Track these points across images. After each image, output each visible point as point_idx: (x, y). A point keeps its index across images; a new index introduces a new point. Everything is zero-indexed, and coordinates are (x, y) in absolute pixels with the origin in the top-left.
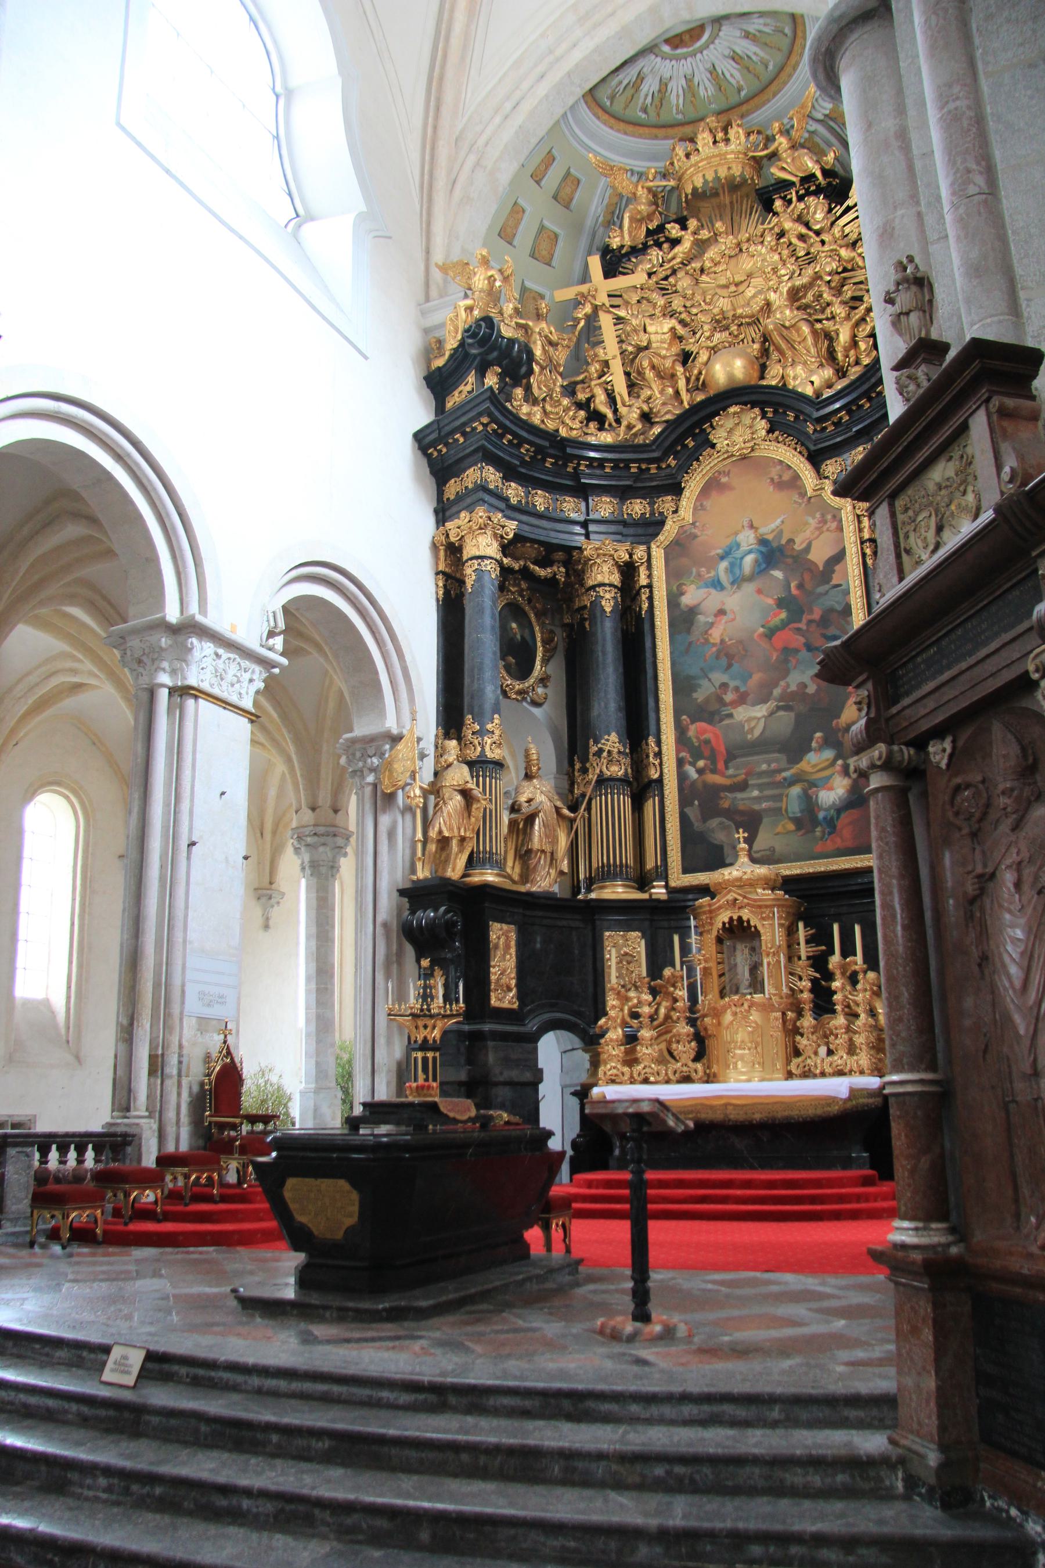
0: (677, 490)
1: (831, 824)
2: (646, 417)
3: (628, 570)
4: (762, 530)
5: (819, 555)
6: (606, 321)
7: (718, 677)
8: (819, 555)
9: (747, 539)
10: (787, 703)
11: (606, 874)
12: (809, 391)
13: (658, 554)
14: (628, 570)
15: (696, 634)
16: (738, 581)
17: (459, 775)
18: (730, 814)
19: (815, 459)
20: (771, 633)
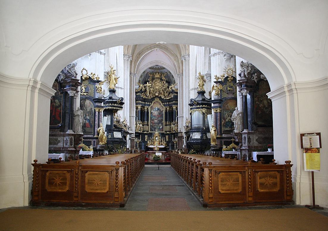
0: (152, 103)
1: (161, 129)
2: (150, 97)
3: (147, 108)
4: (158, 107)
5: (162, 110)
6: (148, 87)
7: (154, 118)
8: (162, 110)
9: (157, 108)
10: (158, 120)
11: (145, 131)
12: (162, 98)
13: (150, 107)
14: (147, 108)
15: (152, 114)
16: (156, 111)
17: (138, 125)
18: (154, 128)
19: (162, 103)
20: (158, 115)
